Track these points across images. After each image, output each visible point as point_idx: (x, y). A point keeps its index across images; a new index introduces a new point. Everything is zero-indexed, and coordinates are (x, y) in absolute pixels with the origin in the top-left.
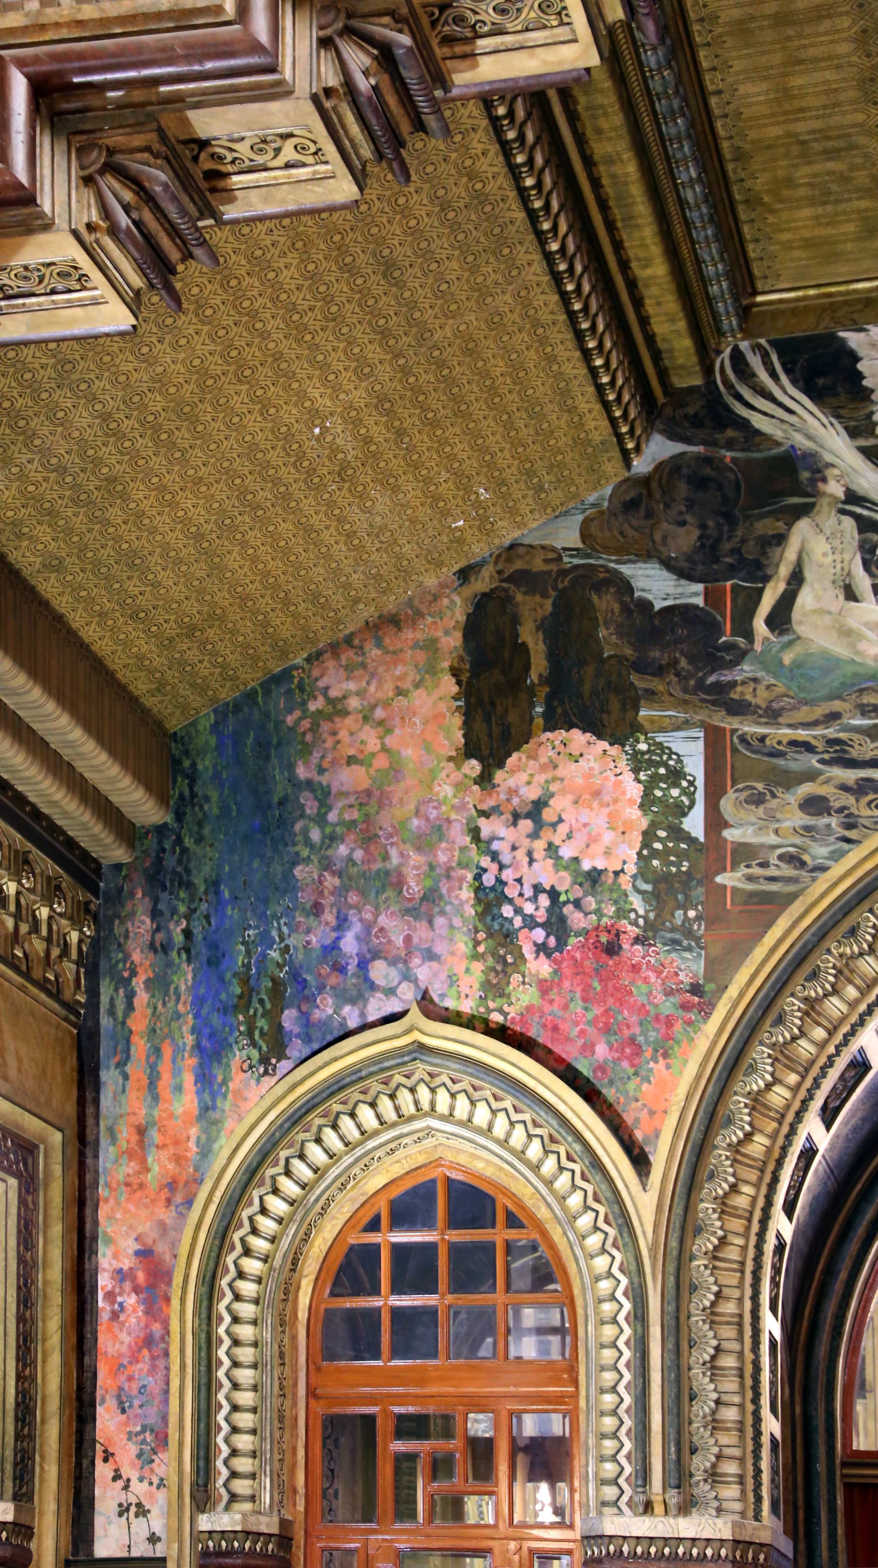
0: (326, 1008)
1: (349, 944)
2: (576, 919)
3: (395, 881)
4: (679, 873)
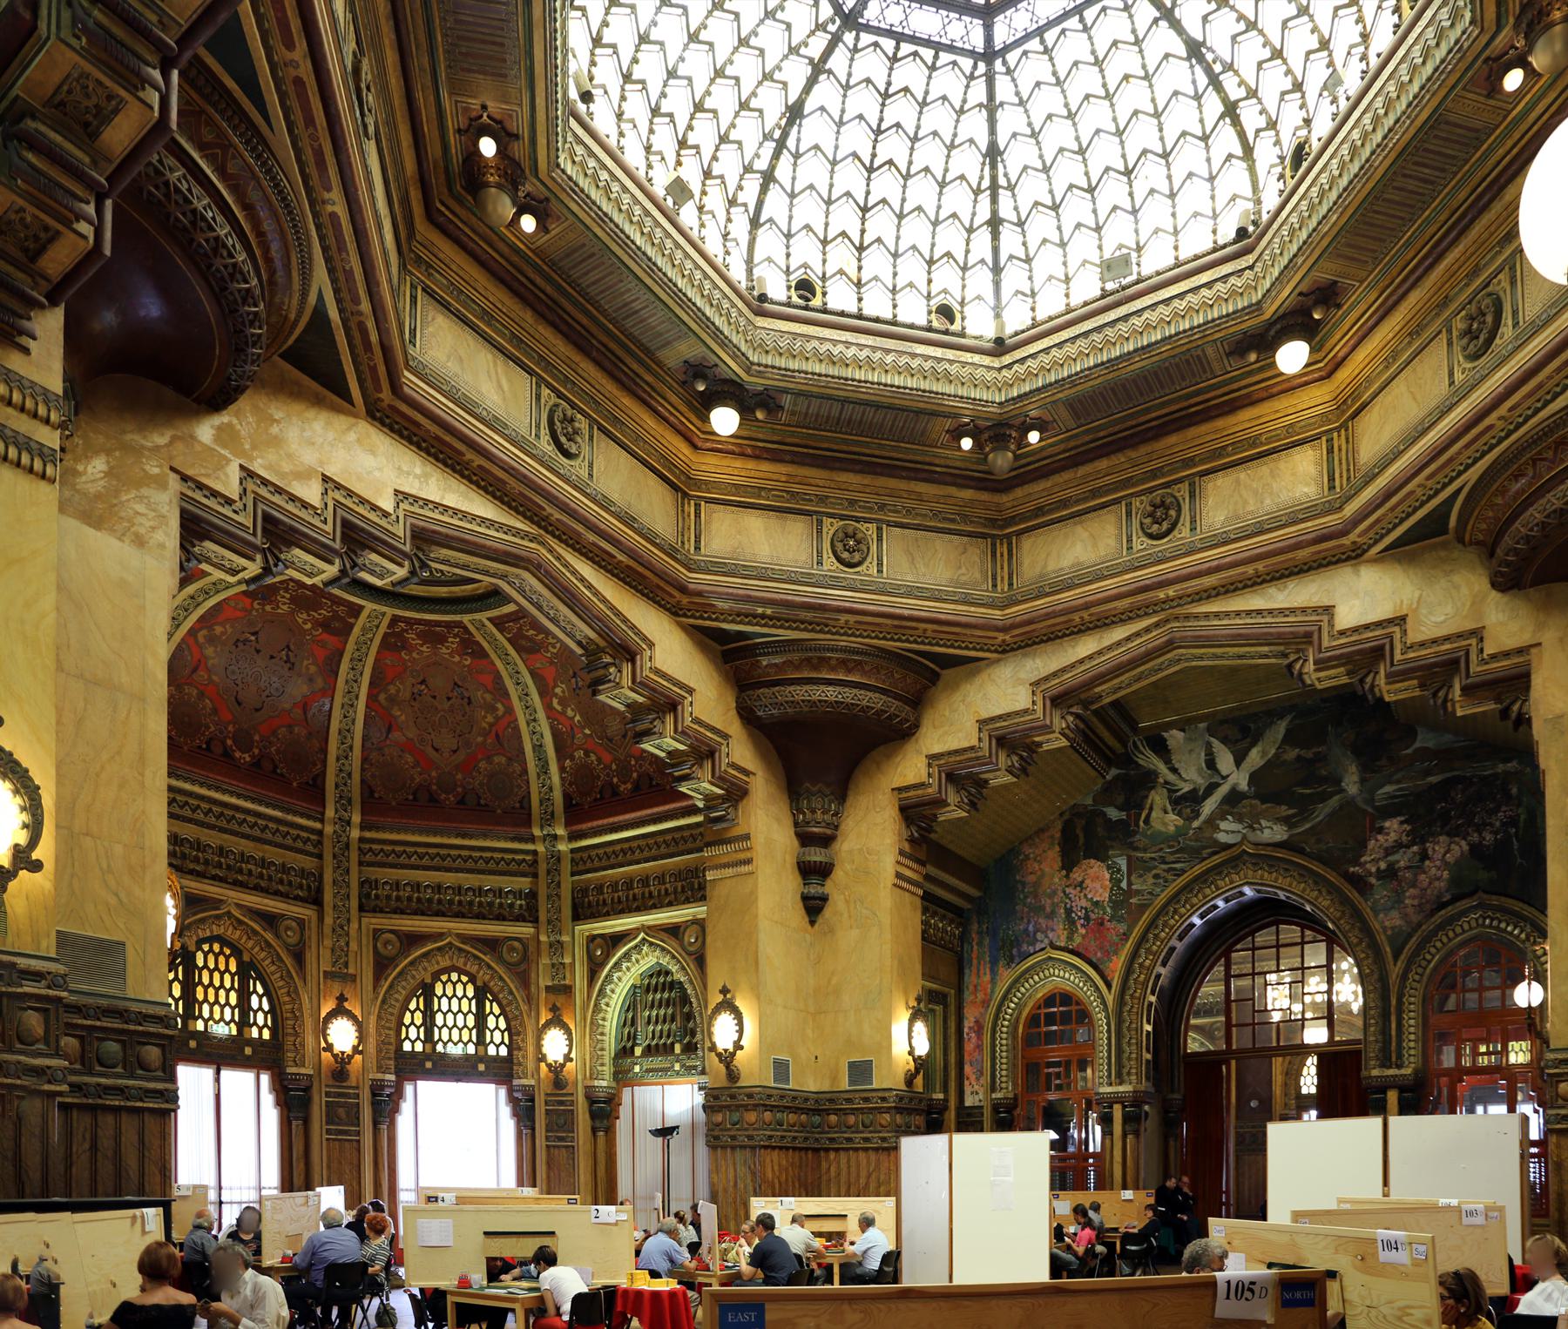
0: (1025, 947)
1: (1031, 928)
2: (1093, 916)
3: (1043, 908)
4: (1121, 899)
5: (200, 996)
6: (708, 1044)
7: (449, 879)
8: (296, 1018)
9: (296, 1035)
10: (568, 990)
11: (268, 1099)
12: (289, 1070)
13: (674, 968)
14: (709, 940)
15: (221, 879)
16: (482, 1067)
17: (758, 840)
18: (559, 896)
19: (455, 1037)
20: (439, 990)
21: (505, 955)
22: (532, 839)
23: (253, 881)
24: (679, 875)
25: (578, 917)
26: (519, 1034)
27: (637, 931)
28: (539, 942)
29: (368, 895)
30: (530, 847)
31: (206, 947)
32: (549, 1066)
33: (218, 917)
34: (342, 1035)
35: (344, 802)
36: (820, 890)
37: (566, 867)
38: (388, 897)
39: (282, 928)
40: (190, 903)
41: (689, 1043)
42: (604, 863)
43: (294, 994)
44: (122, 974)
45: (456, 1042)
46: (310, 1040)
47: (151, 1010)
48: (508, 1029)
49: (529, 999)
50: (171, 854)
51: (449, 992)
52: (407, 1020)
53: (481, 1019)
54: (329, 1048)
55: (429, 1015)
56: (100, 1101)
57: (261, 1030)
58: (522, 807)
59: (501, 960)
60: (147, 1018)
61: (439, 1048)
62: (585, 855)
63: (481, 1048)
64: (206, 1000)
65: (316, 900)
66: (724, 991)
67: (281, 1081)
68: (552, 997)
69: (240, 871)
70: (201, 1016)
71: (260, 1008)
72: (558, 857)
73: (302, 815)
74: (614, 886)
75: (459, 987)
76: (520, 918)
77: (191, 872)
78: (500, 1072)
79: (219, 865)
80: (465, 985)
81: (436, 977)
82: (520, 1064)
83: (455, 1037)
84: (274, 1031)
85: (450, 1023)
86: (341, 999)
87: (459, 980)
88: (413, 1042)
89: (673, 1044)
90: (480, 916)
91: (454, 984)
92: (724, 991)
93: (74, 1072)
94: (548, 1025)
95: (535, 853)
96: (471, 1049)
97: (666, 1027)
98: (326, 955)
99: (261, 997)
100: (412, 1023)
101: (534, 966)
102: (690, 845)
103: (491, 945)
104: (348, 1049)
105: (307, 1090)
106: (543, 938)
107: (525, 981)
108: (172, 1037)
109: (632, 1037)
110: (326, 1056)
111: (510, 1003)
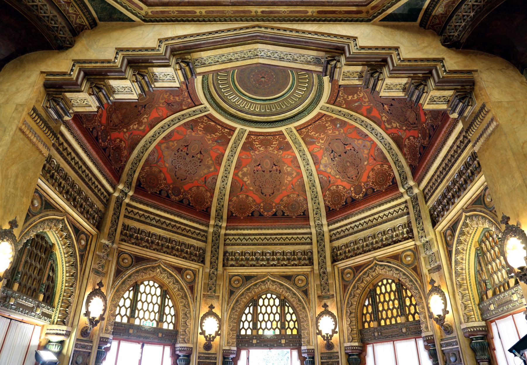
19: (269, 326)
20: (261, 302)
32: (323, 337)
39: (185, 275)
51: (266, 303)
52: (243, 318)
53: (283, 315)
55: (255, 316)
61: (260, 332)
63: (283, 332)
80: (274, 299)
83: (269, 326)
85: (272, 316)
88: (246, 330)
91: (269, 299)
96: (277, 332)
100: (246, 320)
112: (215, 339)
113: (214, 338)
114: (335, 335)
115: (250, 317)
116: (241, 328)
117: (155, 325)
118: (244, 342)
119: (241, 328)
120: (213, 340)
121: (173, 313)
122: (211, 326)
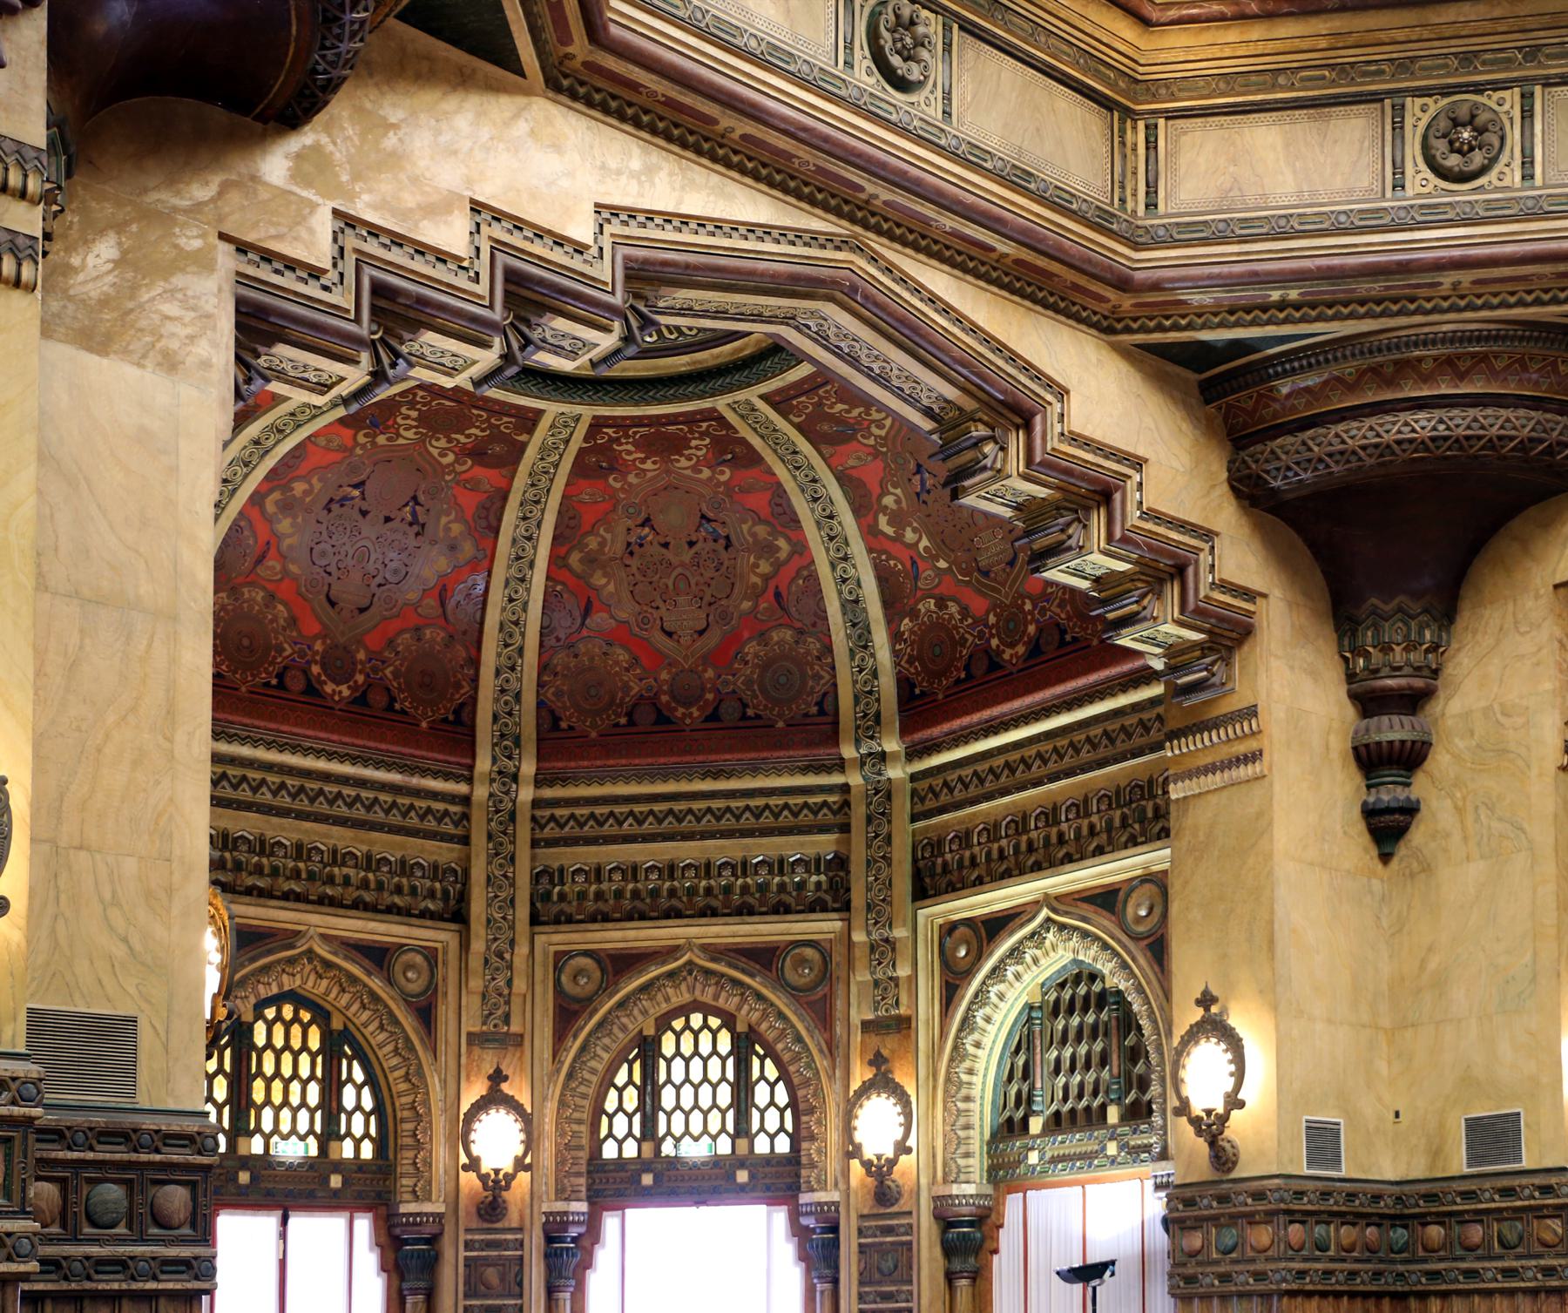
5: (258, 1095)
6: (1173, 1102)
7: (688, 852)
8: (418, 1118)
9: (418, 1146)
10: (903, 1025)
11: (368, 1260)
12: (403, 1209)
13: (1106, 967)
14: (1175, 908)
15: (298, 898)
16: (742, 1176)
17: (1274, 719)
18: (887, 859)
20: (668, 1045)
21: (790, 975)
22: (840, 765)
23: (352, 894)
24: (1115, 797)
25: (923, 892)
26: (811, 1111)
27: (1036, 905)
28: (850, 944)
29: (547, 896)
30: (836, 779)
31: (270, 1013)
32: (867, 1165)
33: (291, 961)
34: (497, 1141)
35: (508, 742)
36: (1401, 794)
37: (902, 806)
38: (582, 896)
39: (398, 968)
40: (246, 942)
41: (1136, 1103)
42: (973, 791)
43: (415, 1078)
44: (129, 1071)
45: (696, 1138)
46: (440, 1154)
47: (177, 1124)
48: (793, 1104)
49: (831, 1048)
50: (216, 865)
51: (687, 1049)
52: (611, 1103)
54: (474, 1164)
55: (649, 1091)
56: (88, 1285)
57: (358, 1145)
58: (822, 712)
59: (782, 983)
60: (170, 1139)
61: (667, 1148)
62: (937, 782)
63: (742, 1144)
64: (268, 1101)
65: (458, 916)
66: (1206, 1000)
67: (390, 1228)
68: (874, 1041)
69: (331, 880)
70: (258, 1129)
71: (358, 1107)
72: (885, 792)
73: (436, 775)
74: (992, 830)
75: (705, 1038)
76: (816, 907)
77: (249, 891)
78: (779, 1181)
79: (296, 875)
80: (715, 1033)
81: (664, 1024)
82: (813, 1165)
84: (381, 1145)
86: (497, 1077)
87: (706, 1026)
88: (620, 1143)
89: (1103, 1107)
90: (745, 911)
91: (696, 1034)
92: (1206, 1000)
93: (50, 1240)
94: (866, 1089)
95: (845, 788)
97: (1091, 1077)
98: (472, 1004)
99: (359, 1088)
100: (620, 1108)
101: (840, 990)
102: (1137, 741)
103: (763, 957)
104: (507, 1166)
105: (433, 1240)
106: (859, 937)
107: (823, 1014)
108: (207, 1168)
109: (1025, 1101)
110: (469, 1180)
111: (796, 1058)
112: (514, 1184)
113: (510, 1178)
114: (903, 1158)
115: (631, 1099)
116: (602, 1135)
117: (314, 1152)
118: (614, 1186)
119: (602, 1135)
120: (508, 1187)
121: (368, 1102)
122: (497, 1141)
